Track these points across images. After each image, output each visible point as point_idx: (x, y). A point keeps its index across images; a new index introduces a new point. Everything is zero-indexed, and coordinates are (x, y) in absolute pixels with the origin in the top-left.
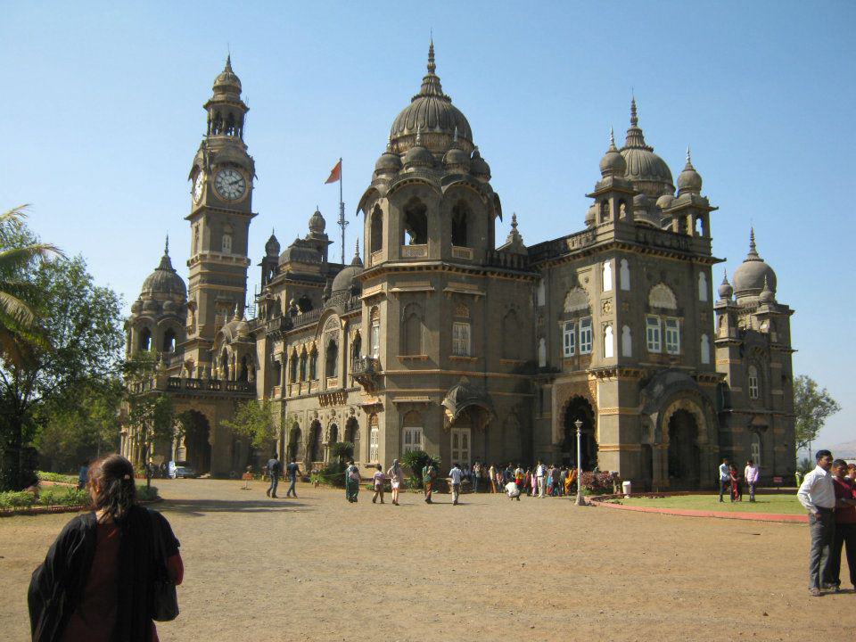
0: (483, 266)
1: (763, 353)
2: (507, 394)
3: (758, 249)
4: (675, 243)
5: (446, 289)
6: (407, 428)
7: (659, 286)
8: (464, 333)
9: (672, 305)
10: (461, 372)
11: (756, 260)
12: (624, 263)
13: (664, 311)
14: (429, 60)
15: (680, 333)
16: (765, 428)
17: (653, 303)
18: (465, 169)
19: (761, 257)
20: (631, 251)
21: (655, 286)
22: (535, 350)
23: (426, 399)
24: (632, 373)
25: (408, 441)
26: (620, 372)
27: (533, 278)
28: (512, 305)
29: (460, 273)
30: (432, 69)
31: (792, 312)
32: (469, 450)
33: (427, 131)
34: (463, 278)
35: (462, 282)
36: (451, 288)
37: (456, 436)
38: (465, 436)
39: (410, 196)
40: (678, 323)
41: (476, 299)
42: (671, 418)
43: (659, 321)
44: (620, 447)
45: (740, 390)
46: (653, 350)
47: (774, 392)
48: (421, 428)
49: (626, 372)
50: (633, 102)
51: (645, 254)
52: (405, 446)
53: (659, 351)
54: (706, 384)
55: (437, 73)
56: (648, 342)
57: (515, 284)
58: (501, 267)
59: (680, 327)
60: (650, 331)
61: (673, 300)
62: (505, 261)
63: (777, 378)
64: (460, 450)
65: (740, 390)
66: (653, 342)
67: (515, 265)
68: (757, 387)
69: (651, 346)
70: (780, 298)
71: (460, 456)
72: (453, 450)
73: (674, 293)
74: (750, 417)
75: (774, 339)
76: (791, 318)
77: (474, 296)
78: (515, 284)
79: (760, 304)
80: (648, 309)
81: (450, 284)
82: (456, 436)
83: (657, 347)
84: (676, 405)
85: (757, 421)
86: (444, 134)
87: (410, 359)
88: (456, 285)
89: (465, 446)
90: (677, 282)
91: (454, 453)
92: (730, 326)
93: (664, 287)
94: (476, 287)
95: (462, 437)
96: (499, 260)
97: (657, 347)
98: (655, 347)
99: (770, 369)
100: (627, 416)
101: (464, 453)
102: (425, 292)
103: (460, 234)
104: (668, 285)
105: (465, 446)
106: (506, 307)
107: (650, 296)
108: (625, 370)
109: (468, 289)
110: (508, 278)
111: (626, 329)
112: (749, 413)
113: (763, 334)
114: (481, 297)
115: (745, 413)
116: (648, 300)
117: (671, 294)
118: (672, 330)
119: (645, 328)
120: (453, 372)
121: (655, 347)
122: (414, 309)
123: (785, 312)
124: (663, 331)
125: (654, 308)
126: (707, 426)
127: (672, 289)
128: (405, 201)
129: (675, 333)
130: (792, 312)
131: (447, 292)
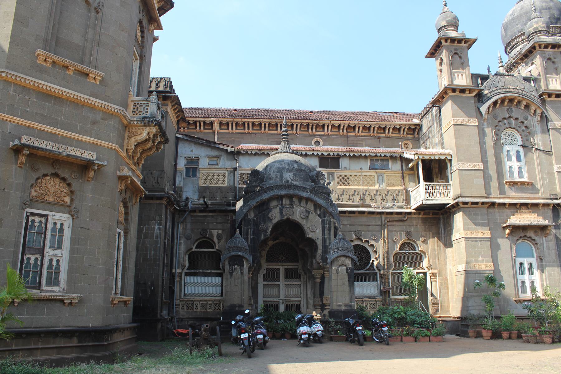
1: (527, 107)
74: (507, 211)
112: (504, 204)
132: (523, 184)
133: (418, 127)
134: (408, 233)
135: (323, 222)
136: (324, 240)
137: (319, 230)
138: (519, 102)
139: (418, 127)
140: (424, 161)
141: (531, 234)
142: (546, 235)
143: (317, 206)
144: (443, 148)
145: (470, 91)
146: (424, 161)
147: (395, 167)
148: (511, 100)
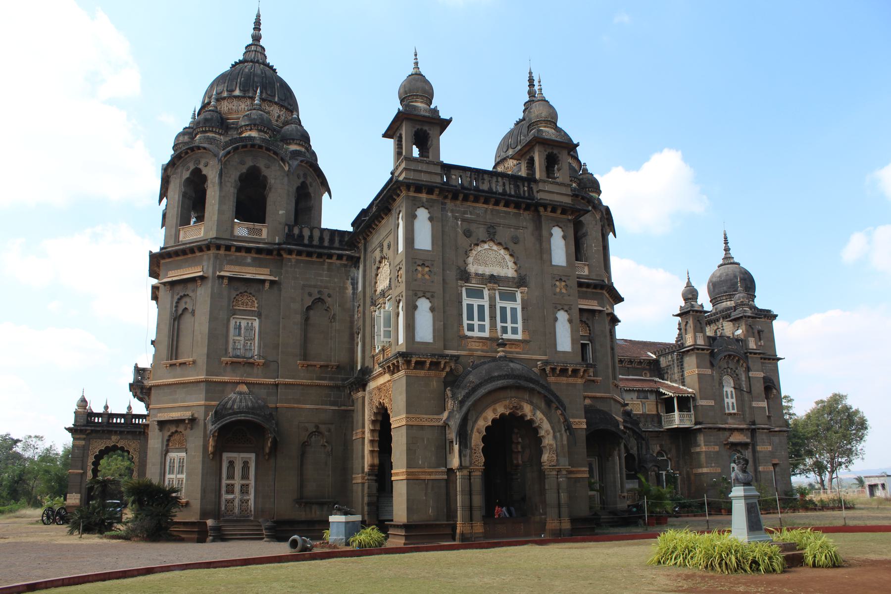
0: (279, 244)
1: (738, 361)
2: (308, 406)
3: (732, 253)
4: (510, 189)
5: (222, 273)
6: (172, 455)
7: (486, 246)
8: (250, 329)
9: (509, 271)
10: (237, 379)
11: (731, 263)
12: (422, 214)
13: (493, 279)
14: (254, 29)
15: (523, 309)
16: (745, 445)
17: (473, 268)
18: (260, 131)
19: (736, 260)
20: (434, 197)
21: (477, 245)
22: (352, 351)
23: (186, 415)
24: (428, 365)
25: (171, 472)
26: (408, 363)
27: (350, 258)
28: (319, 292)
29: (243, 254)
30: (257, 38)
31: (775, 316)
32: (252, 482)
33: (225, 94)
34: (249, 260)
35: (248, 265)
36: (228, 271)
37: (231, 464)
38: (246, 465)
39: (192, 167)
40: (519, 296)
41: (267, 285)
42: (488, 428)
43: (486, 293)
44: (408, 473)
45: (712, 403)
46: (476, 333)
47: (754, 404)
48: (184, 454)
49: (417, 363)
50: (530, 73)
51: (458, 202)
52: (168, 476)
53: (486, 334)
54: (563, 380)
55: (262, 43)
56: (466, 322)
57: (326, 267)
58: (305, 245)
59: (523, 300)
60: (470, 307)
61: (511, 264)
62: (311, 237)
63: (759, 388)
64: (237, 482)
65: (712, 403)
66: (476, 322)
67: (326, 244)
68: (734, 400)
69: (471, 328)
70: (761, 302)
71: (237, 489)
72: (225, 482)
73: (511, 255)
74: (727, 433)
75: (752, 344)
76: (774, 322)
77: (263, 281)
78: (326, 267)
79: (735, 308)
80: (465, 276)
81: (227, 267)
82: (231, 464)
83: (482, 328)
84: (498, 410)
85: (736, 438)
86: (244, 97)
87: (175, 365)
88: (232, 268)
89: (245, 476)
90: (516, 240)
91: (228, 485)
92: (695, 331)
93: (495, 248)
94: (267, 271)
95: (241, 465)
96: (301, 236)
97: (482, 328)
98: (478, 330)
99: (749, 378)
100: (422, 427)
101: (242, 485)
102: (193, 280)
103: (250, 204)
104: (499, 244)
105: (245, 476)
106: (310, 295)
107: (470, 260)
108: (414, 360)
109: (250, 272)
110: (314, 259)
111: (424, 305)
112: (724, 429)
113: (738, 340)
114: (272, 283)
115: (720, 429)
116: (466, 264)
117: (507, 257)
118: (509, 305)
119: (461, 302)
120: (226, 379)
121: (478, 330)
122: (186, 303)
123: (769, 316)
124: (492, 307)
125: (477, 274)
126: (555, 437)
127: (506, 249)
128: (186, 175)
129: (514, 310)
130: (775, 316)
131: (222, 277)
132: (735, 414)
133: (656, 362)
134: (661, 446)
135: (638, 444)
136: (639, 455)
137: (635, 448)
138: (735, 357)
139: (656, 362)
140: (678, 398)
141: (739, 448)
142: (747, 449)
143: (634, 432)
144: (683, 384)
145: (708, 350)
146: (678, 398)
147: (652, 398)
148: (730, 356)
